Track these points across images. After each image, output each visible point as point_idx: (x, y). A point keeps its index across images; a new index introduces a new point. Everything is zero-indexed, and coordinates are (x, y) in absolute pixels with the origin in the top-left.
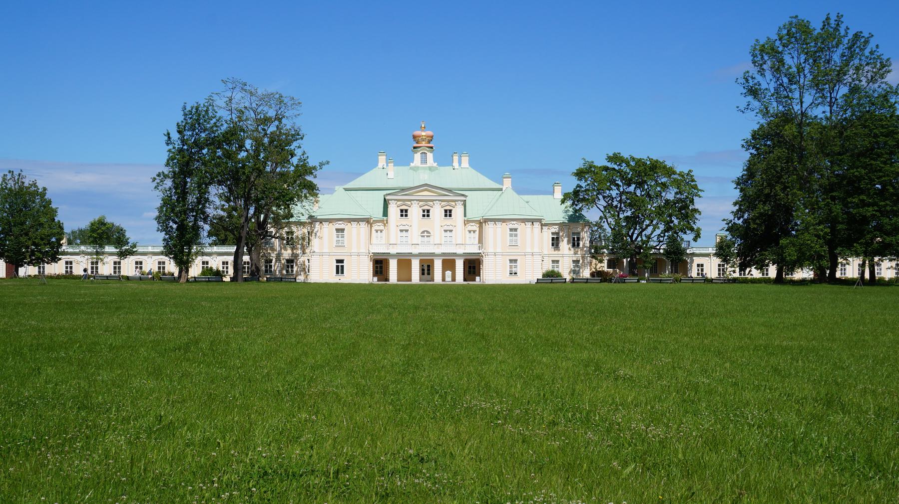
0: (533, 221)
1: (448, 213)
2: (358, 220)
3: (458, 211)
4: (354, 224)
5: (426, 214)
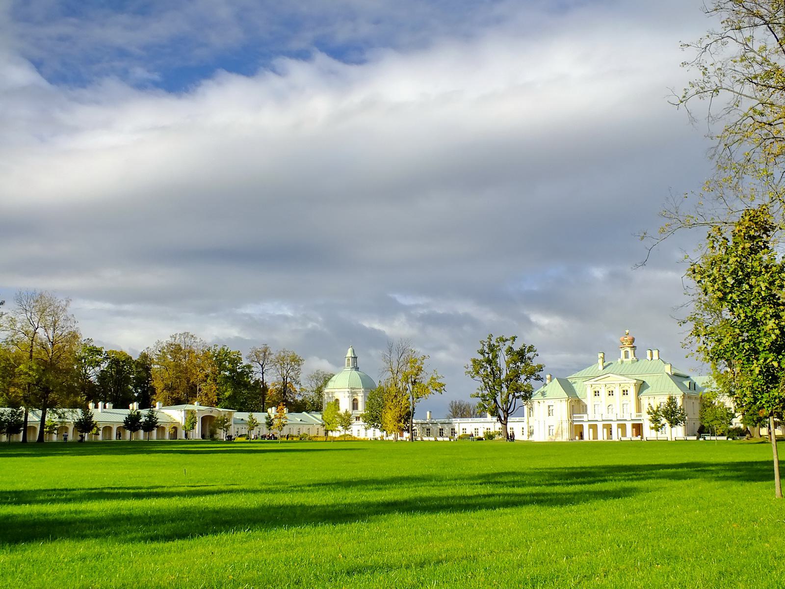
1: (625, 392)
5: (611, 393)
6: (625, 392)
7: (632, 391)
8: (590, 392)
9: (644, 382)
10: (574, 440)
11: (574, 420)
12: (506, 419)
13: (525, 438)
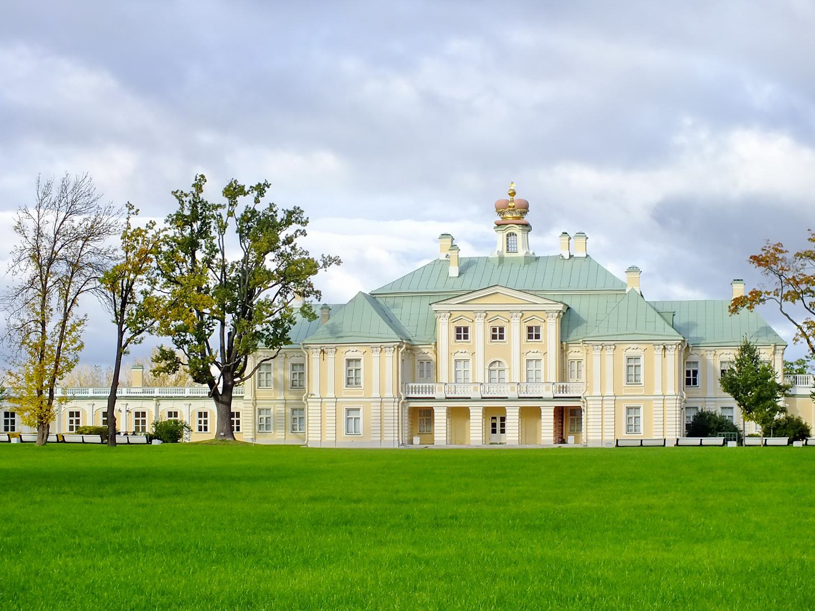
1: (533, 333)
5: (498, 334)
6: (533, 333)
7: (551, 331)
8: (445, 332)
9: (569, 308)
10: (411, 446)
11: (410, 395)
12: (228, 389)
13: (278, 437)
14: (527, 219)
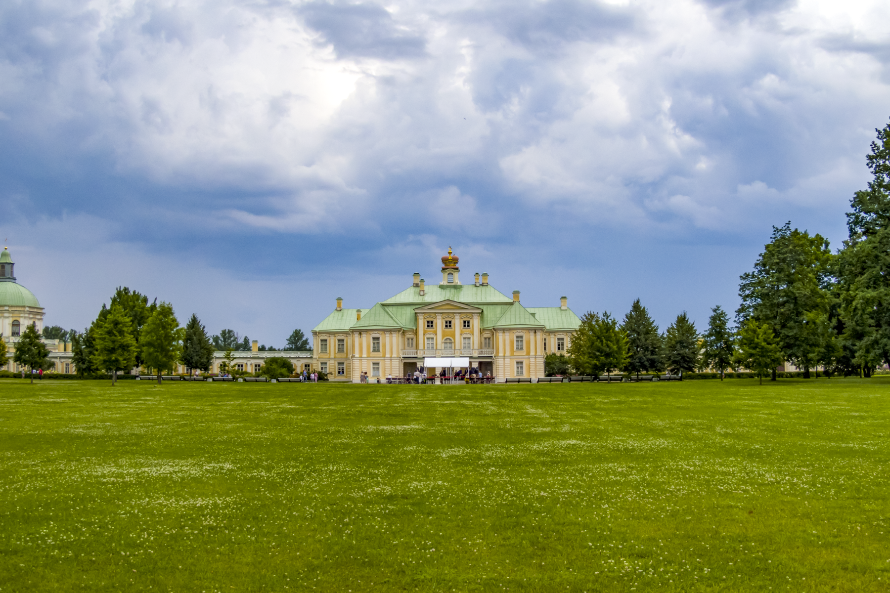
0: (535, 331)
1: (466, 324)
2: (390, 331)
3: (476, 323)
4: (388, 335)
5: (449, 324)
14: (457, 266)
